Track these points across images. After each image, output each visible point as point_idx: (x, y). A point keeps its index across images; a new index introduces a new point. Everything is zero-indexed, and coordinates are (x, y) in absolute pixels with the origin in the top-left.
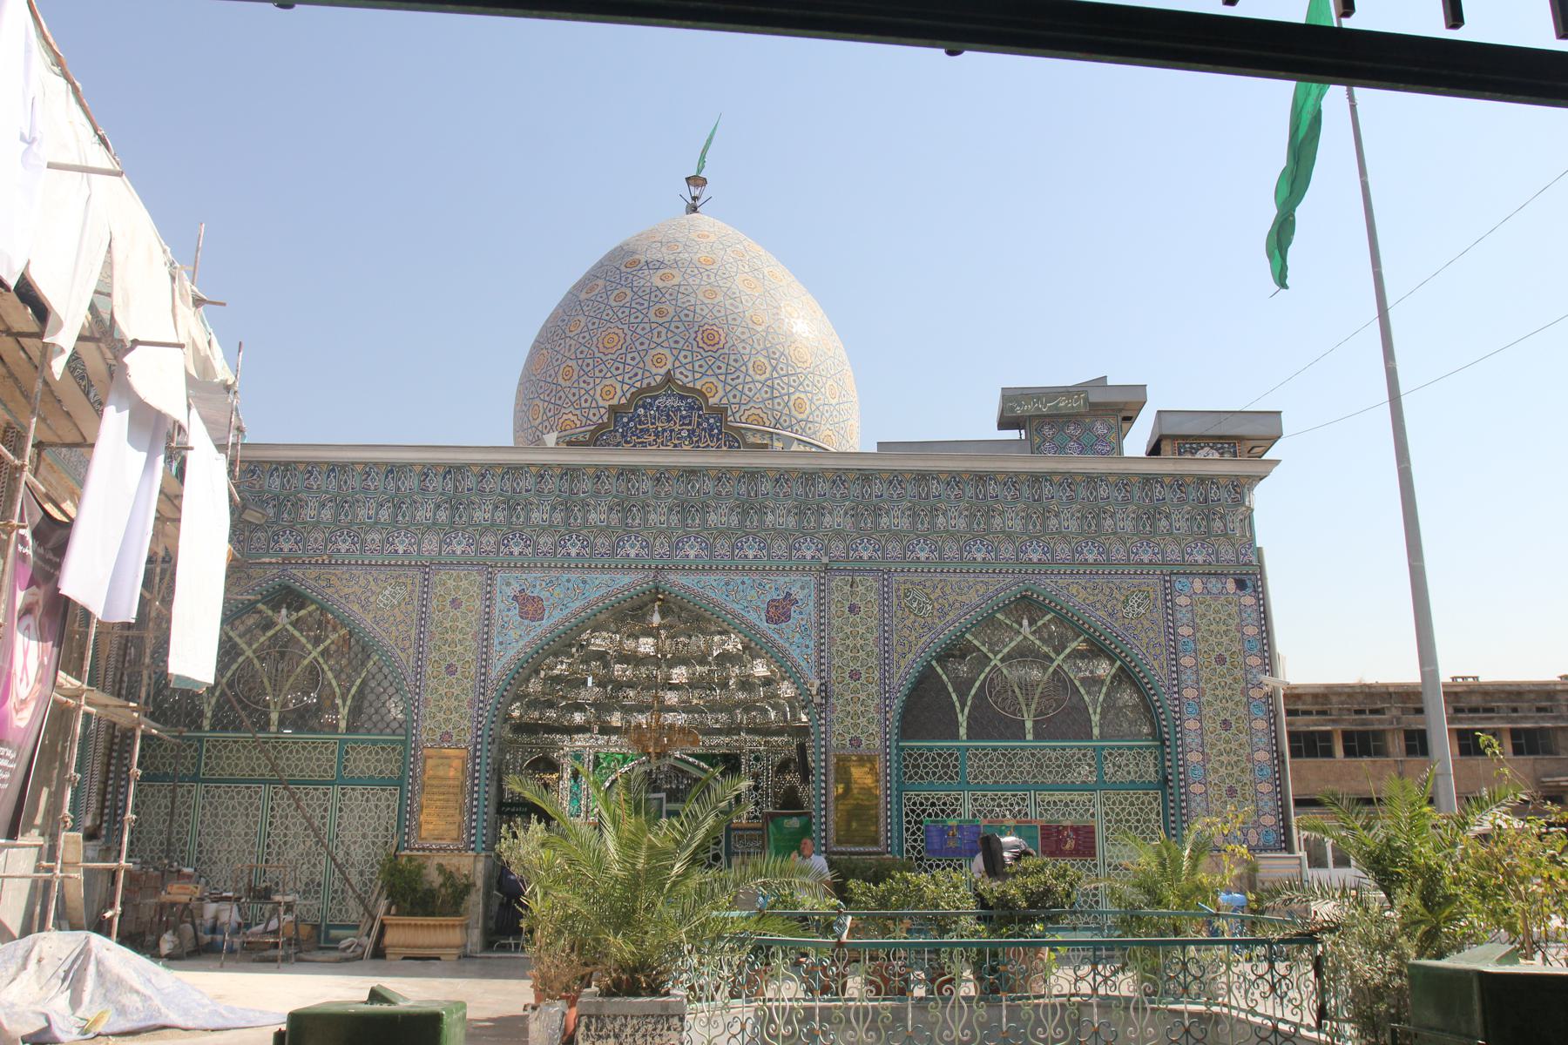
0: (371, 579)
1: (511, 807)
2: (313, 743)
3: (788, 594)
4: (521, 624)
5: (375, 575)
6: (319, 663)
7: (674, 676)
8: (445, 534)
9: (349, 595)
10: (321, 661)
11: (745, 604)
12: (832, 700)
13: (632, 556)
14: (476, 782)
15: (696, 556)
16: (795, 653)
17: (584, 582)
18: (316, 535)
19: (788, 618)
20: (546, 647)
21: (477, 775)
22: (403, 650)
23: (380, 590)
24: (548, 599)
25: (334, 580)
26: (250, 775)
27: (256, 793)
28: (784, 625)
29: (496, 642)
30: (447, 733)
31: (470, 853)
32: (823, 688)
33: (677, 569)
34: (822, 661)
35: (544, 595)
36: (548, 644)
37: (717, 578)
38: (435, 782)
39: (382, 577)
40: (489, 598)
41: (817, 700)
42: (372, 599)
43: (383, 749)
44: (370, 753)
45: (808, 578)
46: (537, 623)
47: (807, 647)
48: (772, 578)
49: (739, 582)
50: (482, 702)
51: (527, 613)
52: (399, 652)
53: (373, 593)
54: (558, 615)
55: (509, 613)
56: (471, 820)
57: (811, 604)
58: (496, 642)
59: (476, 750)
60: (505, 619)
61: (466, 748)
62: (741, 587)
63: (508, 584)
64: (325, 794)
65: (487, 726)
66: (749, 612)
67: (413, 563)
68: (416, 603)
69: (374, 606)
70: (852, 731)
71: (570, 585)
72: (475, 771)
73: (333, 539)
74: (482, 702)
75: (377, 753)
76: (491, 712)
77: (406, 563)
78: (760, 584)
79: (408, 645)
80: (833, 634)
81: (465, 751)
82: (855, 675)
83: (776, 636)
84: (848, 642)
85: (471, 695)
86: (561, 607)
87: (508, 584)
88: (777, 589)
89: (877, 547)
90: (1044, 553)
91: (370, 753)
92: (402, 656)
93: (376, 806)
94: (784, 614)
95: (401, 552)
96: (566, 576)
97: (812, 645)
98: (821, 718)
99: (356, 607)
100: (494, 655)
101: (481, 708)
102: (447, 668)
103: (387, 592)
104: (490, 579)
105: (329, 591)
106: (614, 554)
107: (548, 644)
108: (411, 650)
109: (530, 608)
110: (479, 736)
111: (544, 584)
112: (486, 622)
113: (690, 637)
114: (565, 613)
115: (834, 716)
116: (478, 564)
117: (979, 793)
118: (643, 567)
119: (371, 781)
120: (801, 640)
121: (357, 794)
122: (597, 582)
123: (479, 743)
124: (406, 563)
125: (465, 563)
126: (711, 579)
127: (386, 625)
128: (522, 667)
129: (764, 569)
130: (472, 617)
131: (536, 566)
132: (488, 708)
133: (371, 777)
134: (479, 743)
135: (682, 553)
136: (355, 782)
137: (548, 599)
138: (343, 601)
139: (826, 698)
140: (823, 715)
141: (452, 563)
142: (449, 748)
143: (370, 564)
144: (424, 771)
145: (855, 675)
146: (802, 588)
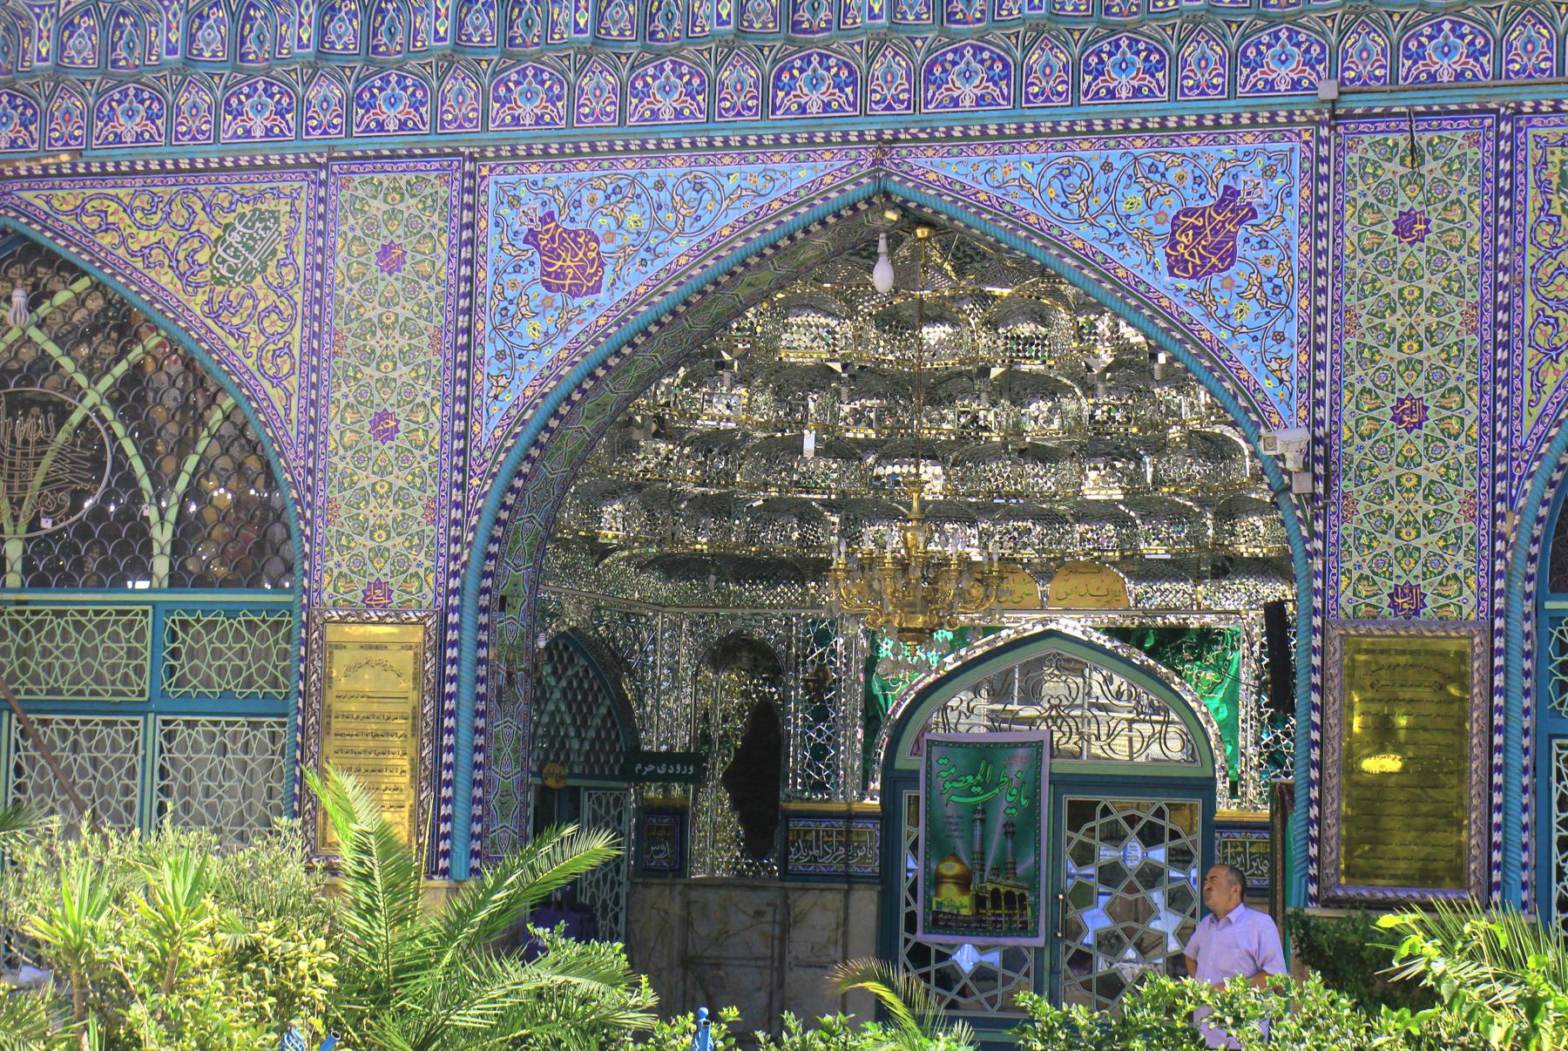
0: (198, 207)
1: (658, 764)
2: (97, 613)
3: (1231, 193)
4: (546, 305)
5: (207, 195)
6: (103, 420)
7: (1029, 426)
8: (99, 95)
9: (151, 247)
10: (107, 412)
11: (1113, 226)
12: (1346, 485)
13: (814, 109)
14: (449, 705)
15: (980, 100)
16: (1247, 360)
17: (699, 187)
18: (194, 97)
19: (1230, 257)
20: (613, 362)
21: (450, 688)
22: (276, 381)
23: (218, 232)
24: (611, 236)
25: (116, 216)
26: (116, 693)
27: (129, 736)
28: (1216, 281)
29: (490, 352)
30: (379, 584)
31: (438, 881)
32: (1320, 451)
33: (932, 138)
34: (1320, 375)
35: (603, 222)
36: (617, 353)
37: (1036, 158)
38: (353, 707)
39: (223, 198)
40: (468, 240)
41: (1303, 484)
42: (202, 257)
43: (250, 625)
44: (222, 637)
45: (1285, 146)
46: (584, 302)
47: (1279, 337)
48: (1187, 150)
49: (1096, 166)
50: (457, 505)
51: (560, 274)
52: (266, 384)
53: (204, 239)
54: (635, 280)
55: (519, 277)
56: (440, 801)
57: (1292, 215)
58: (490, 352)
59: (444, 626)
60: (510, 294)
61: (421, 621)
62: (1101, 180)
63: (515, 202)
64: (129, 736)
65: (473, 565)
66: (1121, 246)
67: (290, 160)
68: (300, 260)
69: (207, 273)
70: (1397, 571)
71: (664, 196)
72: (442, 678)
73: (106, 109)
74: (457, 505)
75: (238, 636)
76: (482, 530)
77: (274, 160)
78: (1153, 169)
79: (286, 369)
80: (1350, 299)
81: (419, 631)
82: (1409, 414)
83: (1196, 312)
84: (1390, 321)
85: (432, 491)
86: (643, 254)
87: (515, 202)
88: (1198, 180)
89: (156, 106)
90: (152, 119)
91: (222, 637)
92: (275, 394)
93: (95, 763)
94: (1216, 249)
95: (258, 133)
96: (653, 174)
97: (1292, 332)
98: (1314, 535)
99: (166, 278)
100: (486, 385)
101: (456, 523)
102: (374, 424)
103: (233, 238)
104: (470, 191)
105: (107, 240)
106: (768, 107)
107: (617, 353)
108: (294, 380)
109: (568, 262)
110: (455, 592)
111: (600, 195)
112: (464, 303)
113: (1041, 318)
114: (651, 270)
115: (1347, 529)
116: (441, 154)
117: (97, 718)
118: (845, 139)
119: (225, 705)
120: (1264, 320)
121: (198, 734)
122: (730, 184)
123: (454, 610)
124: (274, 160)
125: (411, 155)
126: (1024, 164)
127: (236, 321)
128: (555, 414)
129: (1163, 126)
130: (430, 293)
131: (578, 152)
132: (474, 520)
133: (227, 694)
134: (454, 610)
135: (369, 120)
136: (193, 707)
137: (611, 236)
138: (140, 265)
139: (1328, 480)
140: (1319, 526)
141: (379, 156)
142: (381, 622)
143: (193, 169)
144: (327, 679)
145: (1409, 414)
146: (1269, 173)
